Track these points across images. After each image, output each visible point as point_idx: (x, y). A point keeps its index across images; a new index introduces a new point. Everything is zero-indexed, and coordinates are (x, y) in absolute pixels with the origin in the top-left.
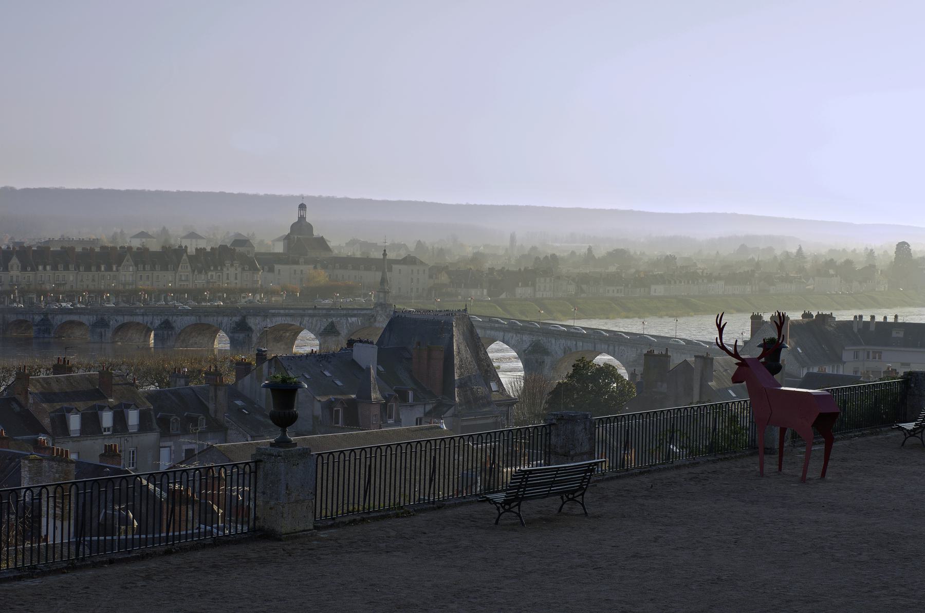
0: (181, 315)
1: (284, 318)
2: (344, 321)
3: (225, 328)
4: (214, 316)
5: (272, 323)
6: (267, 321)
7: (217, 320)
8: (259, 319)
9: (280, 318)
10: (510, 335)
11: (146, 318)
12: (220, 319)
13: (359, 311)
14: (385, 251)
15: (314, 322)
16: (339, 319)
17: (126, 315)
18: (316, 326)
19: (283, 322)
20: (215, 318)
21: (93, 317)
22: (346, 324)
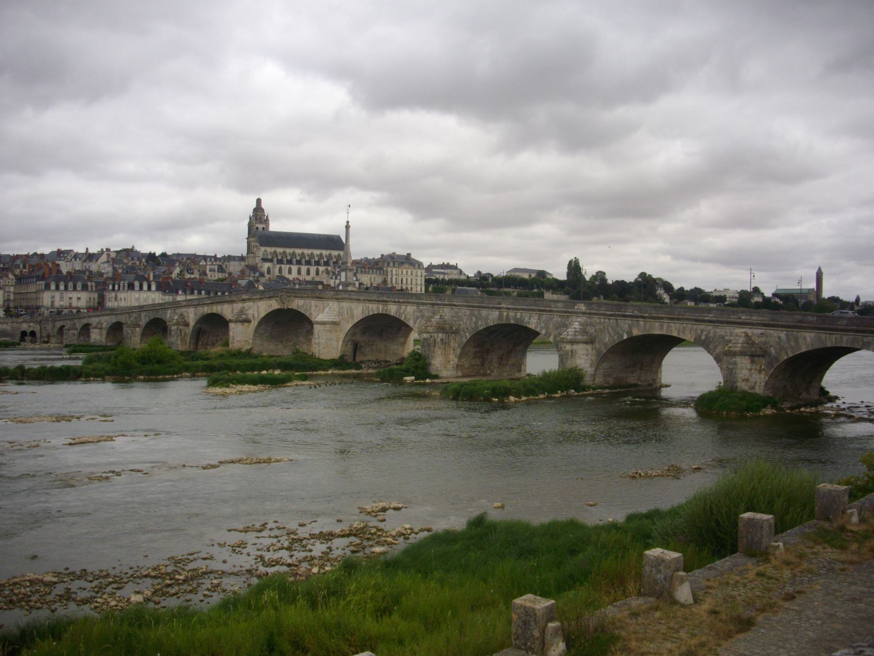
14: (348, 222)
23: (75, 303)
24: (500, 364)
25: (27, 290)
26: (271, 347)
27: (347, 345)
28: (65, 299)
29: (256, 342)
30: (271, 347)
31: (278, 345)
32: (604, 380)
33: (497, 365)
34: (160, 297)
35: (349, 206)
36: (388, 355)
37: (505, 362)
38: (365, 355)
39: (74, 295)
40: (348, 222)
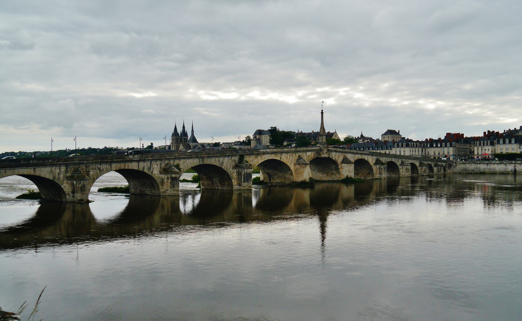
0: (184, 158)
1: (270, 155)
2: (304, 154)
3: (226, 167)
4: (217, 157)
5: (262, 160)
6: (258, 158)
7: (219, 161)
8: (252, 157)
9: (267, 155)
10: (370, 156)
11: (142, 164)
12: (221, 159)
13: (312, 148)
14: (322, 110)
15: (288, 157)
16: (302, 153)
17: (115, 162)
18: (289, 159)
19: (270, 158)
20: (217, 159)
21: (60, 169)
22: (306, 157)
23: (487, 152)
24: (221, 184)
25: (466, 147)
26: (320, 176)
27: (264, 174)
28: (483, 150)
29: (313, 173)
30: (320, 176)
31: (324, 175)
32: (135, 191)
33: (220, 185)
34: (518, 147)
35: (323, 102)
36: (286, 180)
37: (223, 184)
38: (275, 179)
39: (487, 148)
40: (322, 110)
